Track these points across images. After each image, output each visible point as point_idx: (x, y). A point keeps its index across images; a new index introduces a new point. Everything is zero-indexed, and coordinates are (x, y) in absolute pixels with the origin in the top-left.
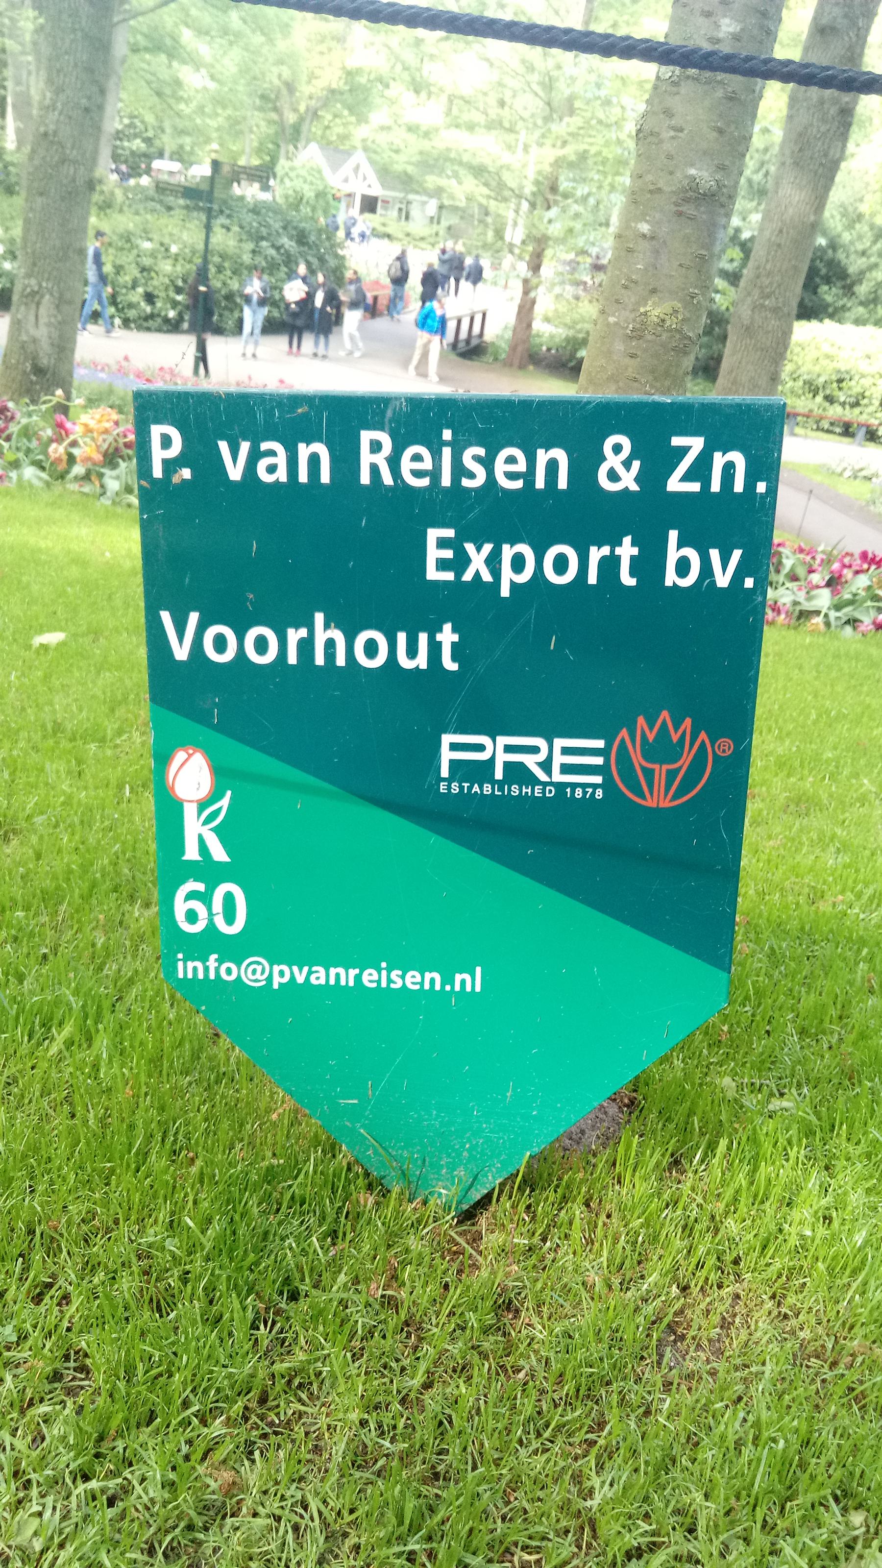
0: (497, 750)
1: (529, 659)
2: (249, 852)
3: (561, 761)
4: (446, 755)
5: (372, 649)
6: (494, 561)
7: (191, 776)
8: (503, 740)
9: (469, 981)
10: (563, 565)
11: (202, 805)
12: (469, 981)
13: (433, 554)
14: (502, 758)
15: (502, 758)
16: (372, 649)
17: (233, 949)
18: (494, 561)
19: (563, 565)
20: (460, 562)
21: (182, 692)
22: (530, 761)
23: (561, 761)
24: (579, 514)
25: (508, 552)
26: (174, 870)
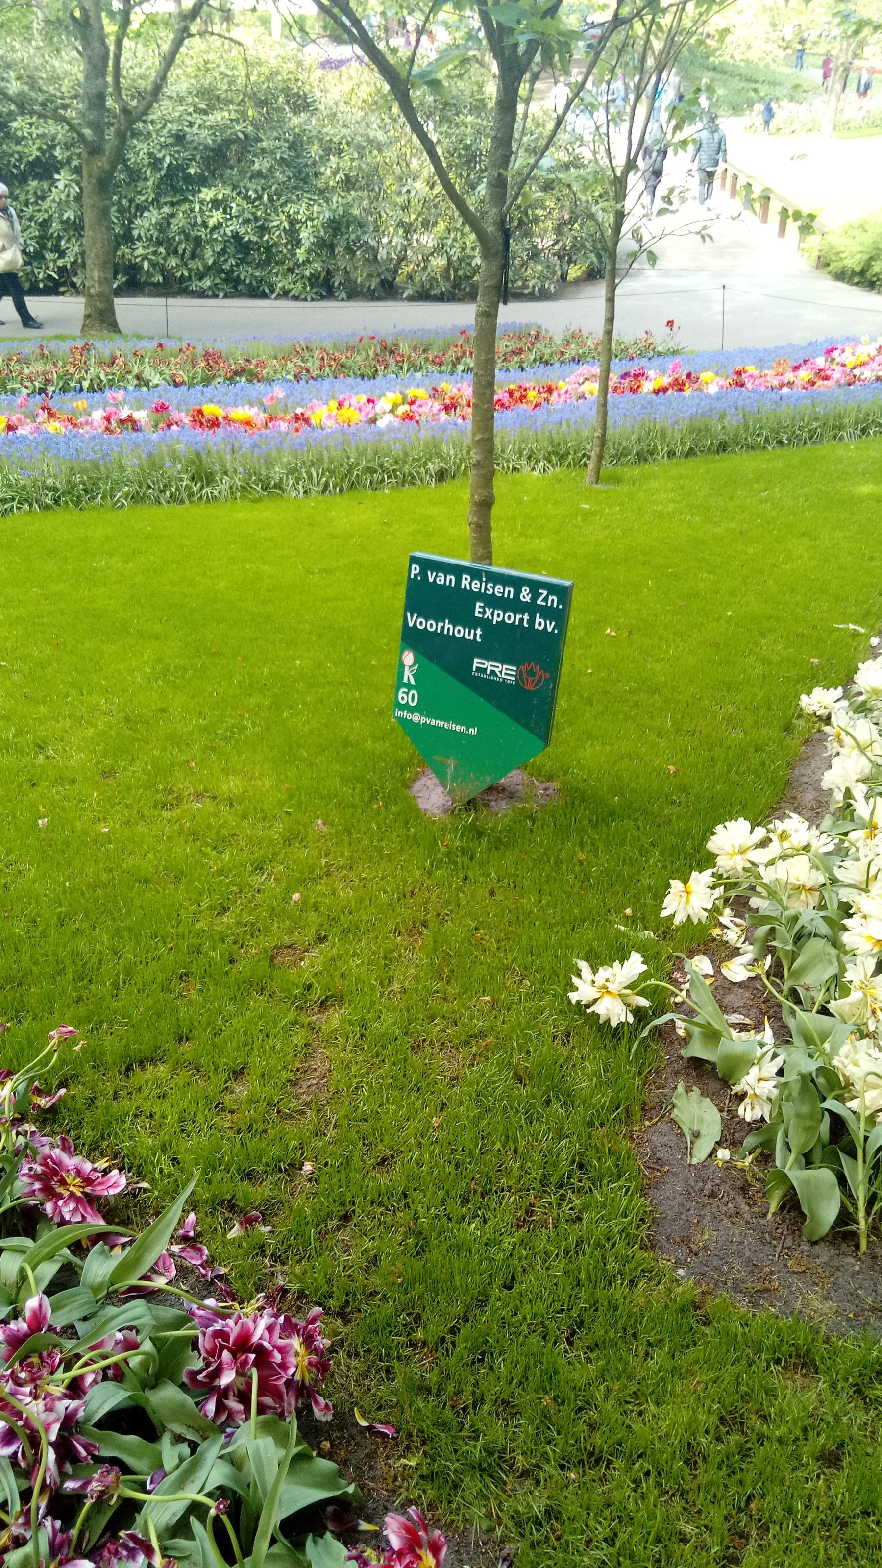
0: (488, 665)
1: (500, 641)
2: (421, 682)
3: (506, 672)
4: (475, 665)
5: (459, 632)
6: (493, 614)
7: (409, 658)
8: (490, 663)
9: (473, 731)
10: (510, 618)
11: (410, 667)
12: (473, 731)
13: (477, 609)
14: (489, 668)
15: (489, 668)
16: (459, 632)
17: (412, 710)
18: (493, 614)
19: (510, 618)
20: (484, 612)
21: (412, 638)
22: (497, 670)
23: (506, 672)
24: (514, 605)
25: (496, 612)
26: (400, 684)
